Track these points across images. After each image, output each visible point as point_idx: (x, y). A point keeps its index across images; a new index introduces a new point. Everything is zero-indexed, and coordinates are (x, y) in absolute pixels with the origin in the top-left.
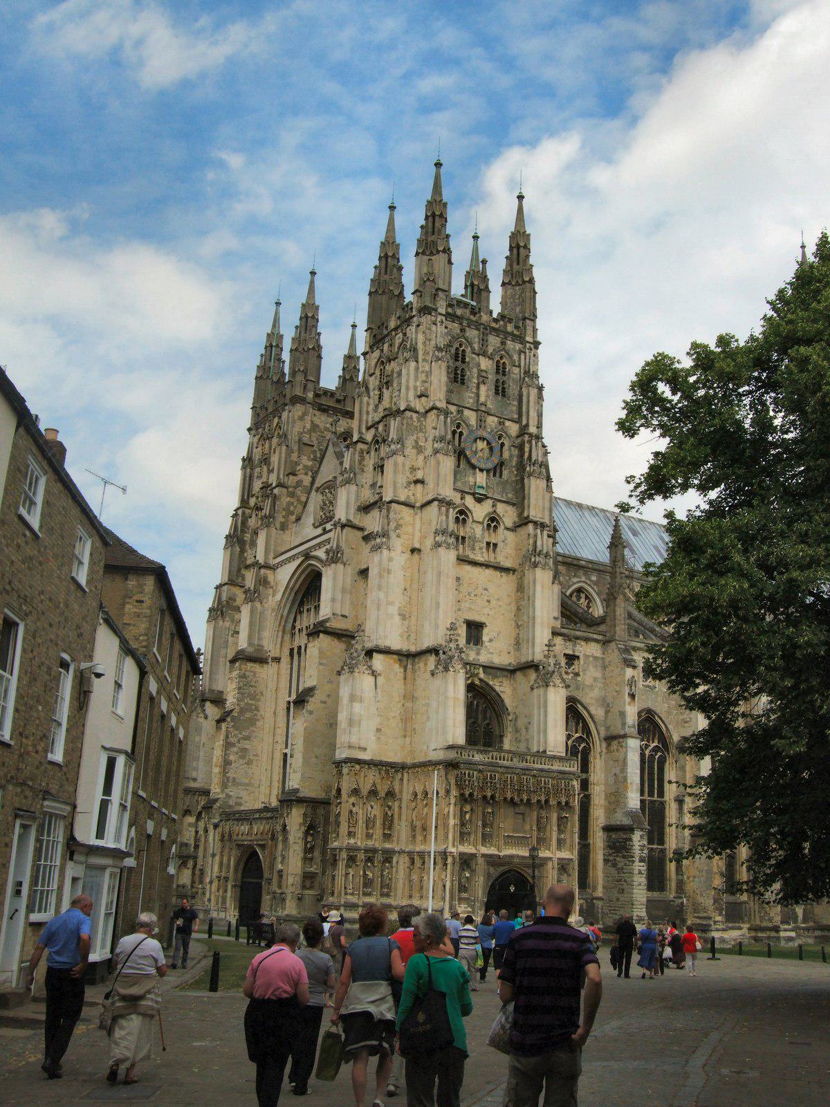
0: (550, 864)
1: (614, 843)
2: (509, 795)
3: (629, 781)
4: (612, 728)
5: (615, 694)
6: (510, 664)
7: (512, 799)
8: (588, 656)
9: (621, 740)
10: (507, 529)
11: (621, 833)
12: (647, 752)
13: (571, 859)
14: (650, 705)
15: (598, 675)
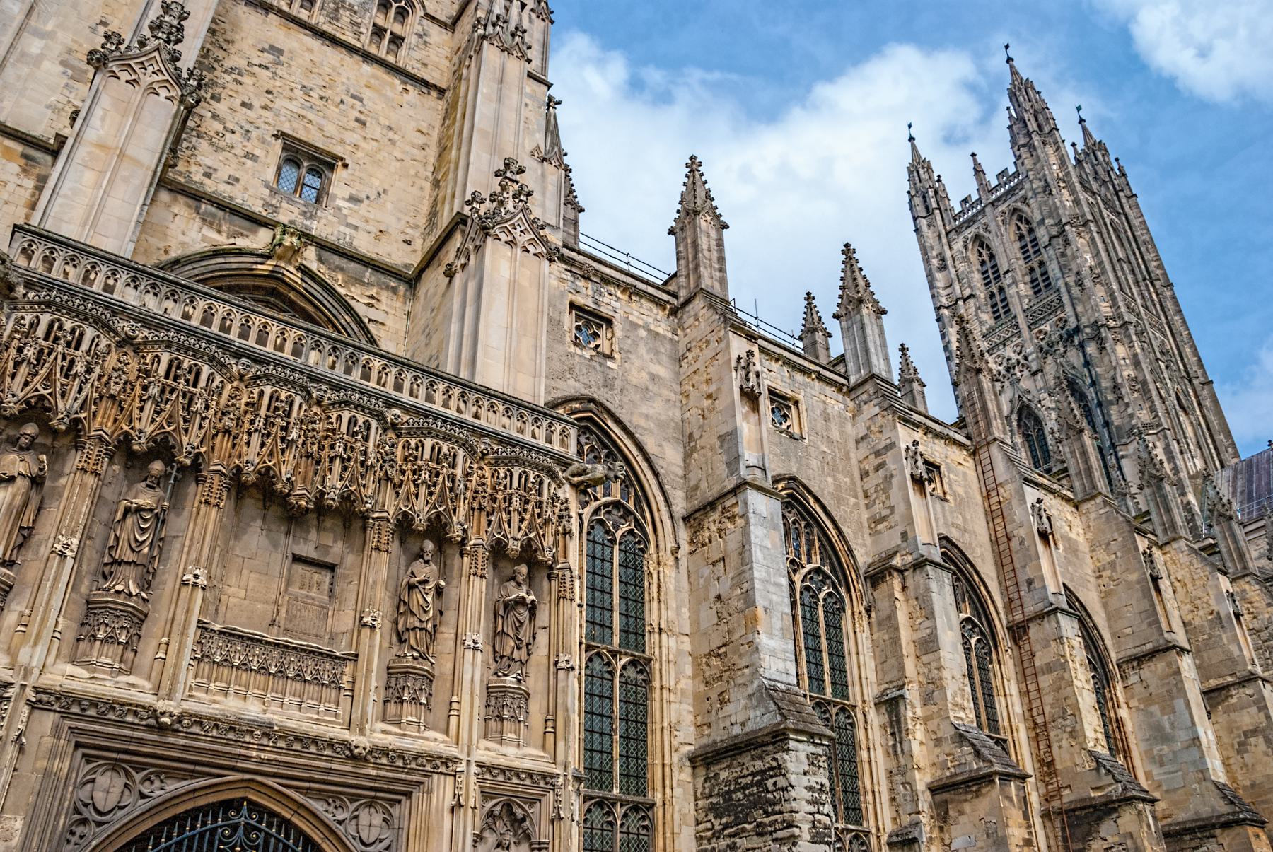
0: (442, 790)
1: (729, 792)
2: (252, 455)
3: (760, 602)
4: (704, 485)
5: (707, 403)
6: (407, 266)
7: (267, 476)
8: (634, 326)
9: (729, 502)
10: (433, 19)
11: (745, 759)
12: (797, 578)
13: (548, 777)
14: (794, 470)
15: (663, 371)
